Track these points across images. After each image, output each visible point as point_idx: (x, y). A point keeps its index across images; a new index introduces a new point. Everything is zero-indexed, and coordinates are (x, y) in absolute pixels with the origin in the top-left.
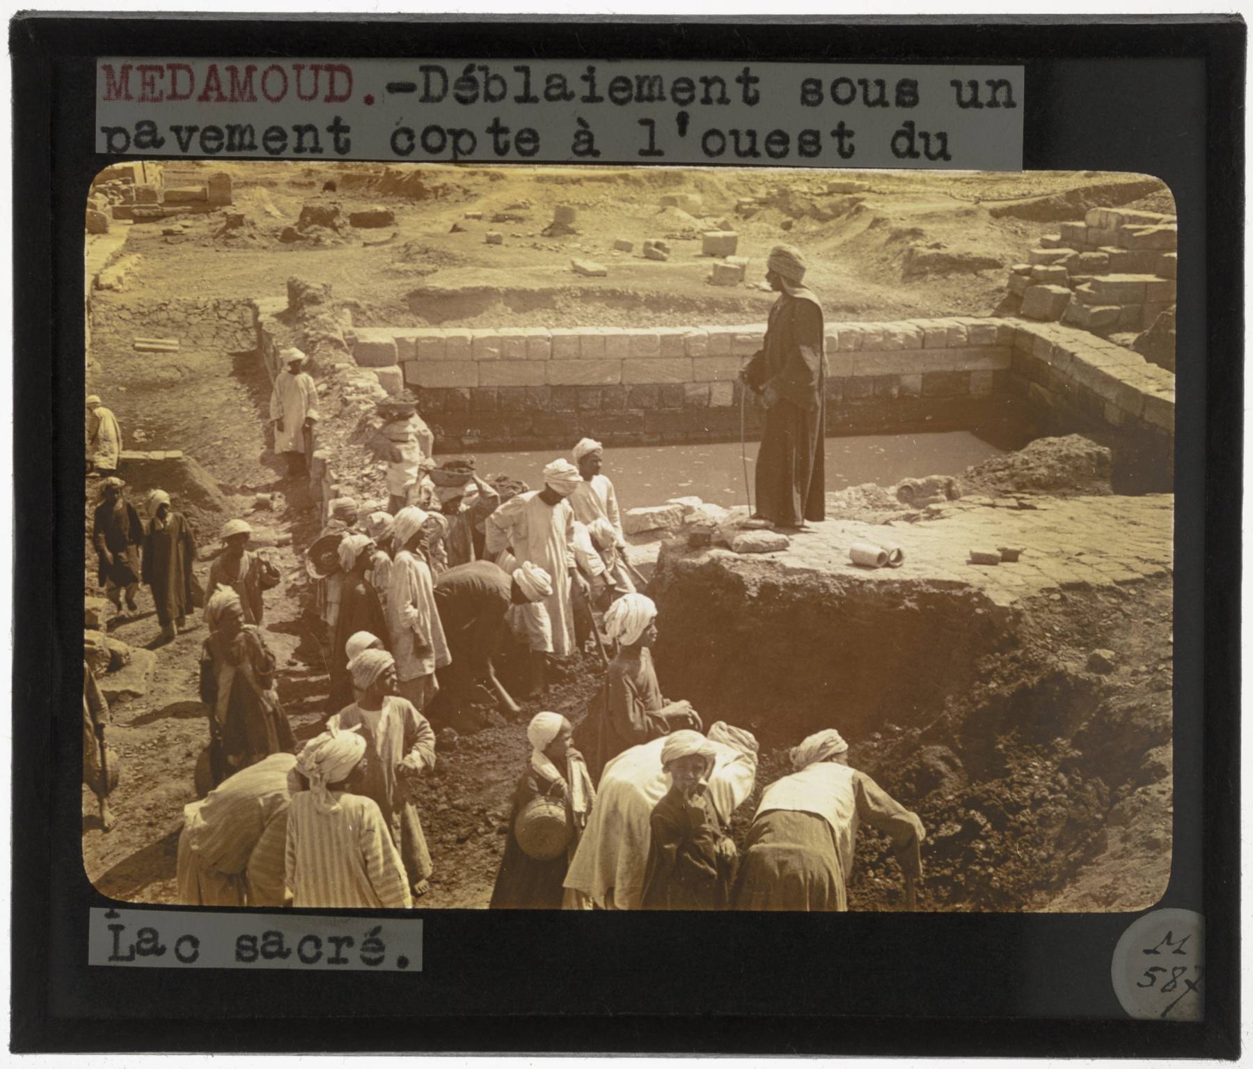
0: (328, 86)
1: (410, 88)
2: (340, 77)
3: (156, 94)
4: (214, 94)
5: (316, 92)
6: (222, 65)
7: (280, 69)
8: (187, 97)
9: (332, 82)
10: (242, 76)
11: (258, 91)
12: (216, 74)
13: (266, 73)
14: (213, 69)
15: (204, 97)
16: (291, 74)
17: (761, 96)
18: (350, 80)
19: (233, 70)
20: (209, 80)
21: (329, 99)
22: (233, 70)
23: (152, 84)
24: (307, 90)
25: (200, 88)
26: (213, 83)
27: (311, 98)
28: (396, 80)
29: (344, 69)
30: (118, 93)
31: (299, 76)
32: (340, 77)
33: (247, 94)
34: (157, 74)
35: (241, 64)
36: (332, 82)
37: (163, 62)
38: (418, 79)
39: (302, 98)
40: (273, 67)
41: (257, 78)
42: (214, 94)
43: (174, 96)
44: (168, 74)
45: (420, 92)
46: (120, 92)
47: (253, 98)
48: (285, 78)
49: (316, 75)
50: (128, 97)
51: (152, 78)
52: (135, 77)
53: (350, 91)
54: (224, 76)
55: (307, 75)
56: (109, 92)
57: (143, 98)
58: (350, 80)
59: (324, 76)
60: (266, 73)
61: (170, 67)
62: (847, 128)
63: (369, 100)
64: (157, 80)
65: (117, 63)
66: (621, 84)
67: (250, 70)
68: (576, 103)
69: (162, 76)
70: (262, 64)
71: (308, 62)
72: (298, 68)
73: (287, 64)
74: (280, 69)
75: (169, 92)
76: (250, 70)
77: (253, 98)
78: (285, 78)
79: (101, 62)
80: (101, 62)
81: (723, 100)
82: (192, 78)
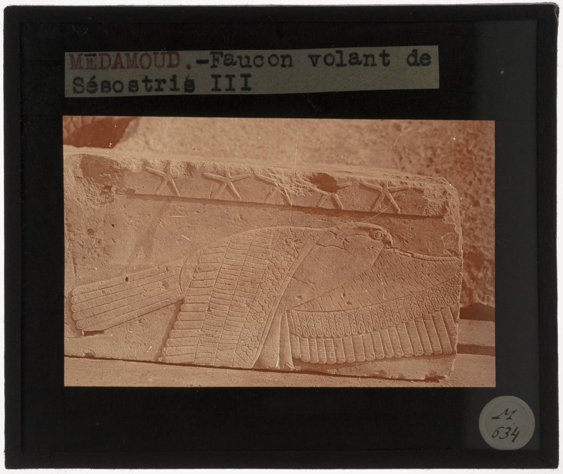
0: (168, 61)
1: (206, 62)
3: (93, 67)
4: (119, 66)
5: (164, 64)
6: (122, 54)
9: (170, 60)
11: (139, 65)
14: (118, 55)
15: (115, 67)
16: (153, 57)
17: (391, 62)
19: (128, 55)
20: (116, 60)
21: (170, 66)
22: (128, 55)
24: (160, 63)
25: (113, 63)
26: (118, 61)
27: (162, 67)
28: (199, 58)
31: (155, 58)
32: (174, 56)
33: (134, 65)
34: (93, 57)
36: (170, 60)
37: (97, 53)
39: (159, 67)
40: (146, 54)
41: (138, 57)
42: (119, 66)
43: (102, 68)
44: (98, 57)
45: (211, 63)
47: (137, 67)
49: (164, 58)
50: (81, 68)
51: (92, 60)
52: (84, 59)
57: (88, 68)
59: (167, 57)
63: (189, 67)
65: (76, 54)
70: (140, 53)
71: (160, 52)
73: (151, 53)
75: (99, 65)
78: (150, 59)
80: (67, 54)
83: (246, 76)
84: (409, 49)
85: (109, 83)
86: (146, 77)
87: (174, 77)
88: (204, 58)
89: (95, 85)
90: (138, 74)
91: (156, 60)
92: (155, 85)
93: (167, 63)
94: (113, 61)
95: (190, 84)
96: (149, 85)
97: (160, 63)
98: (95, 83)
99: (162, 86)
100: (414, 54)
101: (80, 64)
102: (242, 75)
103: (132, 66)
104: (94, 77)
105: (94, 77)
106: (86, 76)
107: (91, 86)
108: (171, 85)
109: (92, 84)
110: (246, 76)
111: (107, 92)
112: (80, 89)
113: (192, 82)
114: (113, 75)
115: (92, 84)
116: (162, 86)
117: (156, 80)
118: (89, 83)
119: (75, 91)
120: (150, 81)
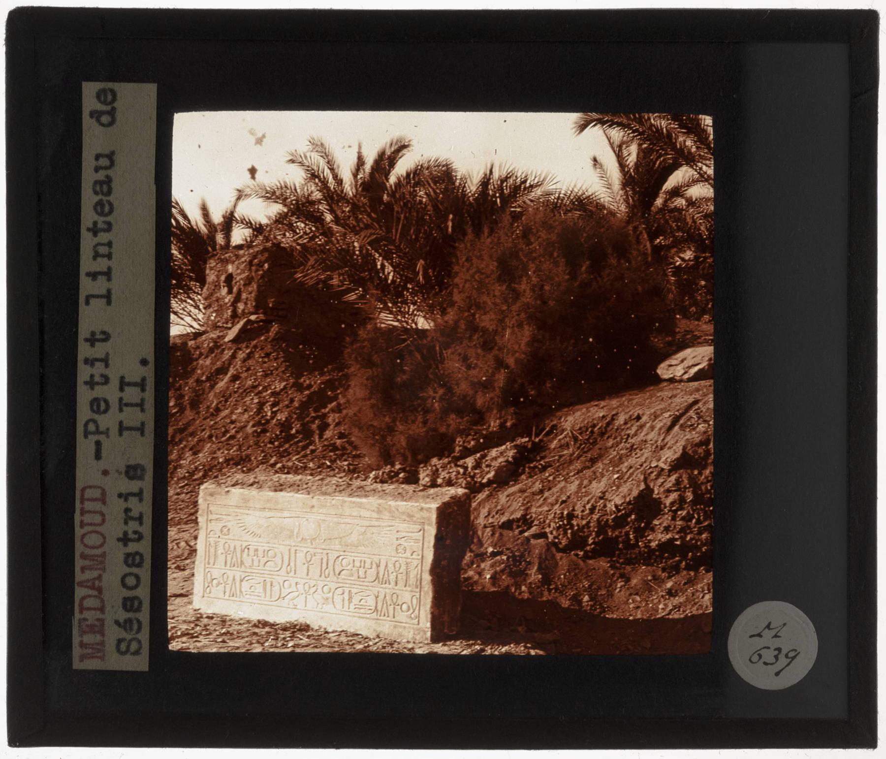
1: (98, 444)
2: (89, 493)
3: (97, 623)
6: (79, 576)
7: (83, 536)
8: (102, 601)
10: (87, 563)
11: (98, 552)
12: (85, 581)
13: (86, 546)
14: (82, 584)
16: (87, 529)
18: (90, 487)
21: (103, 500)
22: (83, 569)
23: (92, 626)
24: (98, 519)
27: (103, 515)
29: (83, 490)
30: (99, 651)
35: (79, 563)
37: (77, 615)
38: (93, 438)
41: (88, 552)
43: (102, 610)
45: (102, 438)
46: (99, 650)
47: (104, 555)
48: (90, 532)
49: (89, 512)
50: (102, 643)
51: (87, 626)
52: (88, 638)
53: (98, 487)
54: (89, 575)
55: (87, 518)
56: (97, 657)
58: (90, 487)
59: (88, 506)
60: (86, 546)
61: (81, 612)
62: (121, 536)
63: (105, 473)
64: (88, 623)
65: (76, 651)
66: (99, 208)
67: (83, 556)
68: (113, 264)
69: (85, 620)
70: (79, 548)
72: (82, 525)
74: (83, 536)
75: (98, 615)
76: (83, 556)
77: (104, 555)
78: (90, 532)
79: (77, 665)
80: (77, 665)
81: (110, 244)
82: (89, 596)
83: (123, 384)
84: (87, 122)
85: (125, 599)
86: (119, 540)
87: (120, 495)
88: (93, 448)
89: (129, 621)
90: (116, 554)
91: (91, 524)
92: (133, 526)
93: (98, 506)
94: (91, 592)
95: (133, 472)
96: (131, 536)
97: (98, 519)
98: (126, 621)
99: (135, 513)
100: (96, 115)
101: (97, 644)
102: (121, 389)
103: (102, 562)
104: (117, 623)
105: (117, 623)
106: (113, 633)
107: (131, 629)
108: (133, 502)
109: (126, 625)
110: (123, 384)
111: (140, 603)
112: (134, 646)
113: (128, 467)
114: (114, 594)
115: (126, 625)
116: (135, 513)
117: (126, 523)
118: (125, 629)
119: (137, 653)
120: (126, 533)
